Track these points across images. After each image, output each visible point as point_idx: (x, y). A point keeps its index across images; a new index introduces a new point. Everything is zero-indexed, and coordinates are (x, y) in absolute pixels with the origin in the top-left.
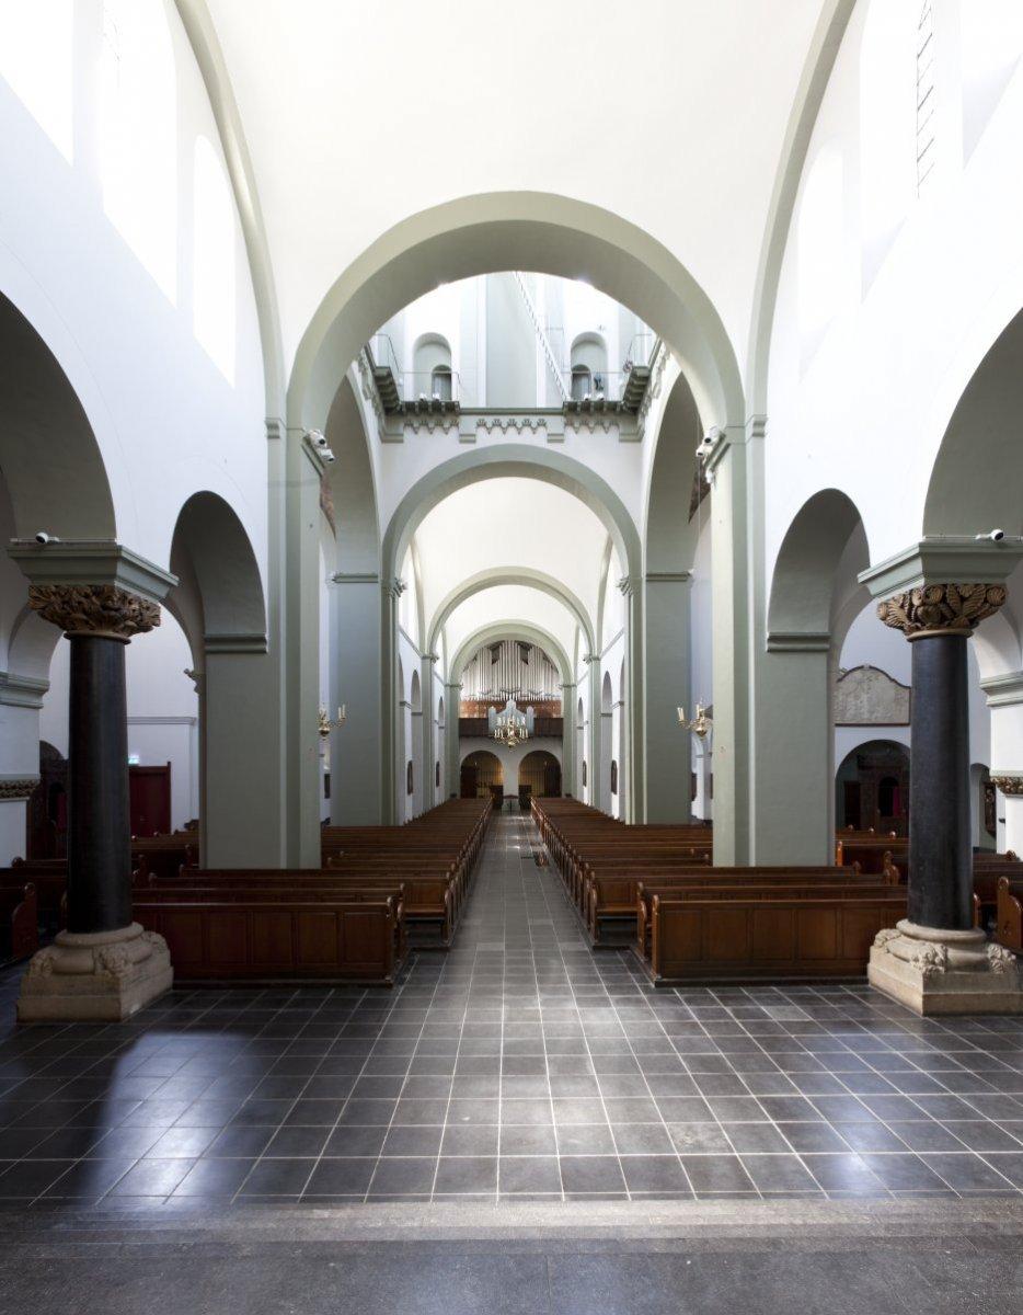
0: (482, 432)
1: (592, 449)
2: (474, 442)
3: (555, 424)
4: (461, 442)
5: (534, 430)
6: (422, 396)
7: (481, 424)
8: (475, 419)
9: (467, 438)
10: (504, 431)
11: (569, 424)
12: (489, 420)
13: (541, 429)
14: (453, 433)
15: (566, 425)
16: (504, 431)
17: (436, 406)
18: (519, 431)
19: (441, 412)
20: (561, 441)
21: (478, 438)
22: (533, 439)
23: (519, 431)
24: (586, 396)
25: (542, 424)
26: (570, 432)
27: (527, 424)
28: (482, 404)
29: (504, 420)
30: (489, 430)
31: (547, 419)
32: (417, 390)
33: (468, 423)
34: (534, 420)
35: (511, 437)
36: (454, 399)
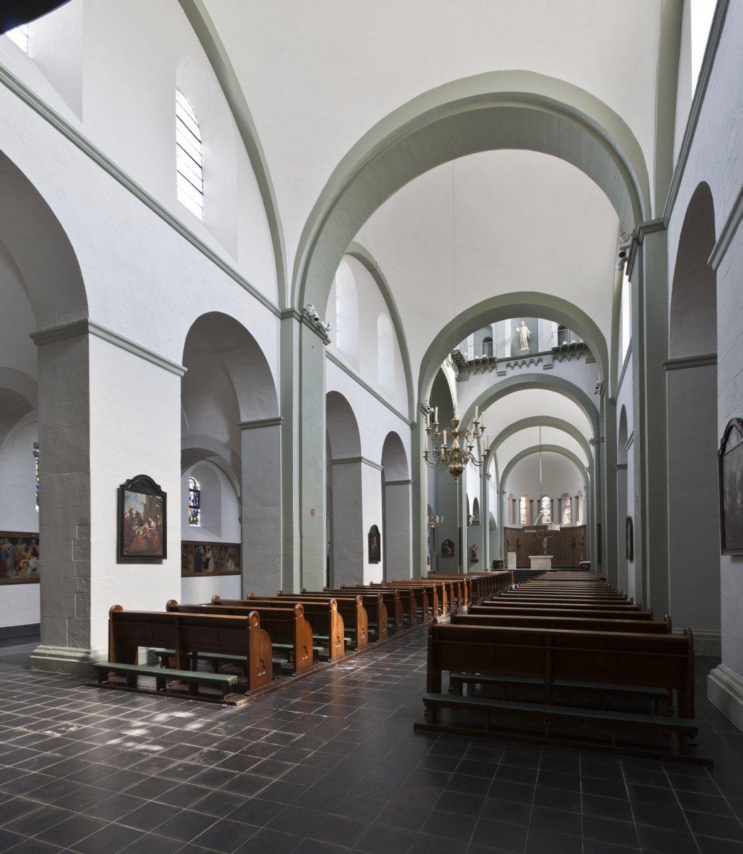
0: (509, 368)
1: (569, 370)
2: (505, 375)
3: (547, 360)
4: (498, 376)
5: (536, 364)
6: (477, 357)
7: (508, 366)
8: (506, 363)
9: (501, 374)
10: (520, 367)
11: (554, 359)
12: (512, 363)
13: (540, 363)
14: (494, 372)
15: (554, 359)
16: (520, 367)
17: (484, 361)
18: (528, 366)
19: (488, 363)
20: (552, 368)
21: (507, 373)
22: (537, 369)
23: (528, 366)
24: (565, 343)
25: (540, 360)
26: (557, 363)
27: (532, 362)
28: (508, 355)
29: (520, 362)
30: (513, 368)
31: (543, 357)
32: (475, 355)
33: (501, 367)
34: (536, 359)
35: (525, 370)
36: (494, 356)
